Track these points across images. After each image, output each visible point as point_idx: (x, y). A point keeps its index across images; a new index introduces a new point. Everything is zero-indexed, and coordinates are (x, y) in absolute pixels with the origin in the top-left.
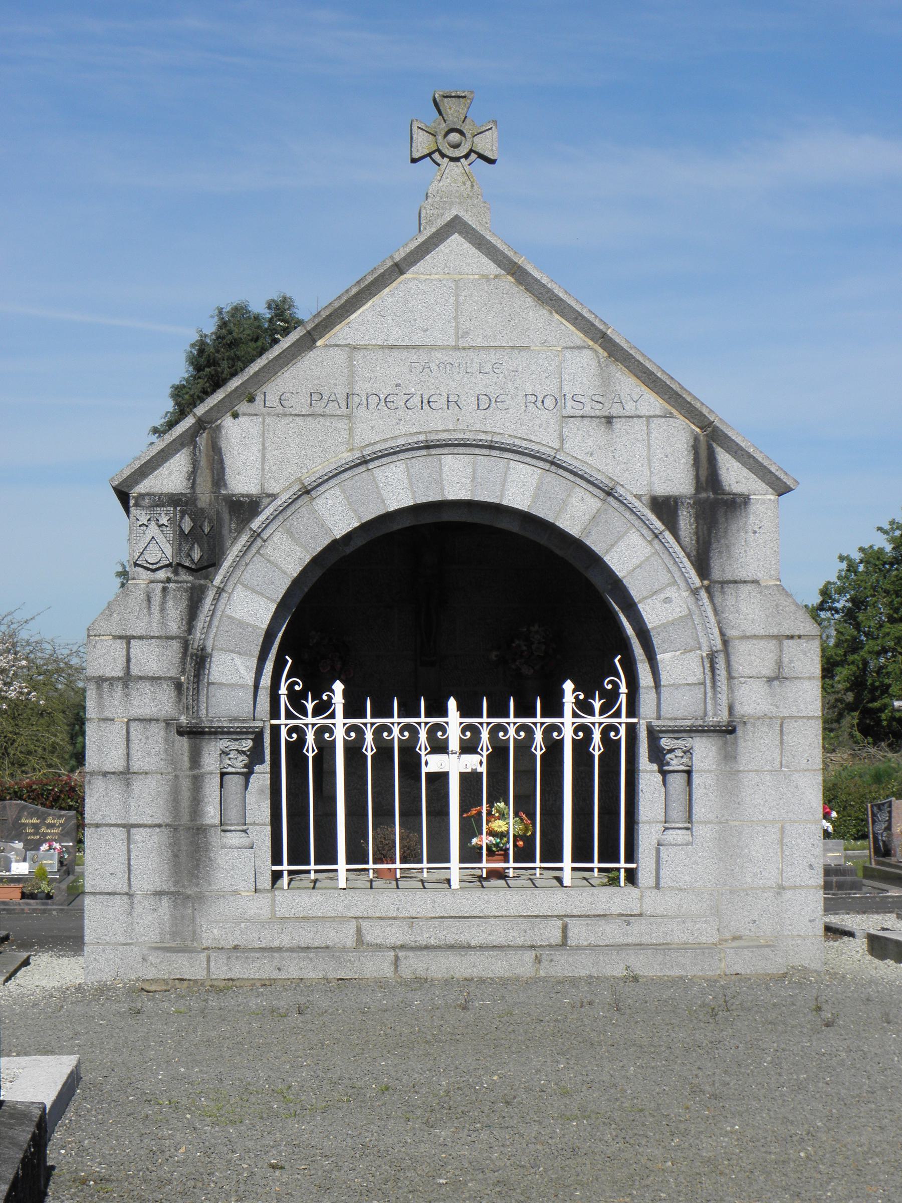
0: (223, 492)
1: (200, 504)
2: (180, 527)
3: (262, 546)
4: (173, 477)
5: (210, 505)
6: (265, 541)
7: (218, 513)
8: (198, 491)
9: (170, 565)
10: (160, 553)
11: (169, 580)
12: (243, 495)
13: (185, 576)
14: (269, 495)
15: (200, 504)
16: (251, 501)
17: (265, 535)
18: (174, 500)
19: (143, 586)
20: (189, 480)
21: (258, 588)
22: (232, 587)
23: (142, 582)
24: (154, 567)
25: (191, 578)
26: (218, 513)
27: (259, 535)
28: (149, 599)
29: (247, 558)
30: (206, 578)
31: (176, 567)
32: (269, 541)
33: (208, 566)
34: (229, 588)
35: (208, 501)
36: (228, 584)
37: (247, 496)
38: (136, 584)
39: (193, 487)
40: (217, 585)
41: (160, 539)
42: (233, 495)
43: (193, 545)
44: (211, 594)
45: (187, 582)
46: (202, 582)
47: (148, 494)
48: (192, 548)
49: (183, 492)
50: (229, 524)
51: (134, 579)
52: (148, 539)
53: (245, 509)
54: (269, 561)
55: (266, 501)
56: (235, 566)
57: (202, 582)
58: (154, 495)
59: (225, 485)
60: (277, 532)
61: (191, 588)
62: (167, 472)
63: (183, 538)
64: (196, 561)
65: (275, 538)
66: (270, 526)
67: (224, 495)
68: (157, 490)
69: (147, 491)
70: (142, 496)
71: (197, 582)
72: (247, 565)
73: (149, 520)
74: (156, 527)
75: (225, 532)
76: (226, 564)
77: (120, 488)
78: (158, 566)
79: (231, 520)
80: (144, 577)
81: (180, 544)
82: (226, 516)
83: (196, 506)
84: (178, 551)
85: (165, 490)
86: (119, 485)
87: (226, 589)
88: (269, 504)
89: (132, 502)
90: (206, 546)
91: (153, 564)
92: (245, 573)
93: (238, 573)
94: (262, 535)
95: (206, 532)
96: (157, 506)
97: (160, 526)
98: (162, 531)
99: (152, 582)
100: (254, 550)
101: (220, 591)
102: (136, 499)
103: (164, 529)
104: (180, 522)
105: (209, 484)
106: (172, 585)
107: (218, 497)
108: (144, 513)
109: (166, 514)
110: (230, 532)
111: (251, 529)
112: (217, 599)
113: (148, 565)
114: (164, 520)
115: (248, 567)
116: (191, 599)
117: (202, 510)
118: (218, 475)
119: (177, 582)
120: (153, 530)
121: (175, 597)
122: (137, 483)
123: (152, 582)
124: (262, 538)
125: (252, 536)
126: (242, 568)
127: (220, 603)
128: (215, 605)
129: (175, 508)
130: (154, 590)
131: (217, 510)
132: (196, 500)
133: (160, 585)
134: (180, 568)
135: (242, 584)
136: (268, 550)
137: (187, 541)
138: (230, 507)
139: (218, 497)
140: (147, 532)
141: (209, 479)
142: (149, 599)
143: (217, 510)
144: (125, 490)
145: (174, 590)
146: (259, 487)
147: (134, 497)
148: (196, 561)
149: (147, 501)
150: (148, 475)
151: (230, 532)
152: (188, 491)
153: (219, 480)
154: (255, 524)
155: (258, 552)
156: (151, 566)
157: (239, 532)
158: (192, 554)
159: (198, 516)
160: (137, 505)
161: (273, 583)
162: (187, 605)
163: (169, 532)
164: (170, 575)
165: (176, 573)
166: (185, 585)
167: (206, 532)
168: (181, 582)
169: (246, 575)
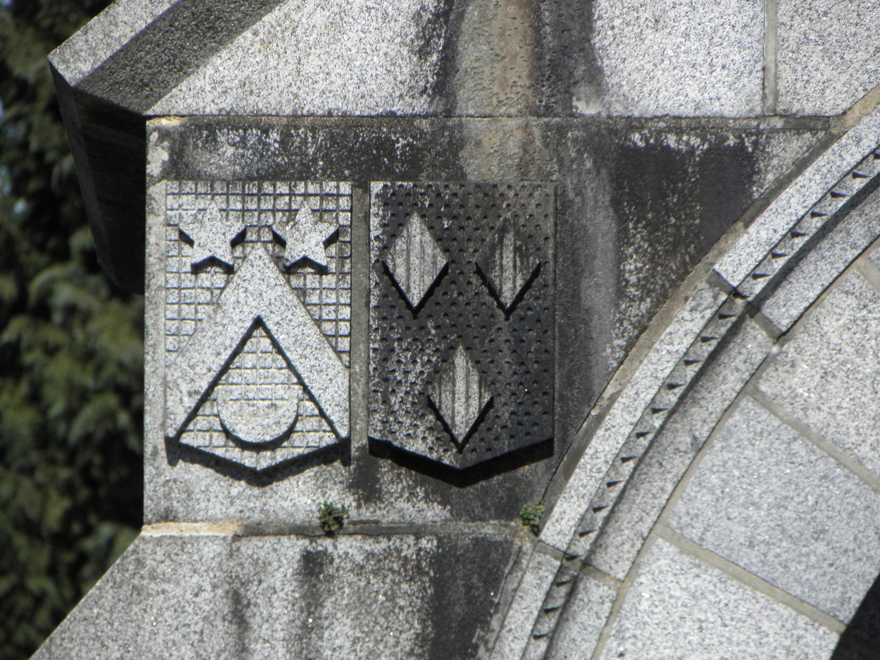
0: (587, 108)
1: (479, 167)
2: (386, 272)
3: (768, 360)
4: (350, 39)
5: (523, 168)
6: (781, 337)
7: (562, 206)
8: (469, 101)
9: (338, 451)
10: (289, 400)
11: (332, 523)
12: (677, 124)
13: (408, 504)
14: (799, 124)
15: (479, 167)
16: (717, 151)
17: (782, 310)
18: (355, 149)
19: (210, 550)
20: (423, 53)
21: (750, 558)
22: (629, 552)
23: (203, 530)
24: (265, 460)
25: (434, 513)
26: (562, 206)
27: (754, 308)
28: (239, 612)
29: (700, 418)
30: (508, 509)
31: (367, 460)
32: (801, 338)
33: (514, 455)
34: (615, 559)
35: (513, 147)
36: (613, 539)
37: (700, 125)
38: (182, 542)
39: (443, 85)
40: (561, 542)
41: (293, 326)
42: (634, 123)
43: (447, 357)
44: (531, 587)
45: (418, 532)
46: (489, 529)
47: (232, 121)
48: (440, 372)
49: (399, 108)
50: (612, 260)
51: (168, 516)
52: (236, 332)
53: (687, 186)
54: (803, 431)
55: (786, 150)
56: (643, 453)
57: (489, 529)
58: (260, 123)
59: (595, 77)
60: (836, 297)
61: (439, 560)
62: (320, 18)
63: (404, 327)
64: (461, 430)
65: (830, 325)
66: (807, 266)
67: (588, 123)
68: (275, 97)
69: (227, 103)
70: (204, 128)
71: (468, 530)
72: (699, 447)
73: (239, 240)
74: (272, 273)
75: (597, 293)
76: (603, 447)
77: (99, 91)
78: (281, 455)
79: (623, 238)
80: (216, 509)
81: (386, 354)
82: (599, 223)
83: (460, 176)
84: (377, 385)
85: (314, 102)
86: (98, 75)
87: (602, 560)
88: (801, 166)
89: (157, 158)
90: (506, 359)
91: (258, 447)
92: (690, 488)
93: (658, 484)
94: (769, 309)
95: (508, 297)
96: (276, 175)
97: (289, 270)
98: (302, 293)
99: (254, 530)
100: (730, 378)
101: (574, 572)
102: (179, 143)
103: (311, 280)
104: (385, 248)
105: (520, 72)
106: (347, 548)
107: (561, 130)
108: (214, 207)
109: (320, 214)
110: (621, 293)
111: (717, 281)
112: (558, 610)
113: (235, 454)
114: (308, 241)
115: (707, 460)
116: (436, 610)
117: (489, 193)
118: (561, 29)
119: (371, 530)
120: (259, 288)
121: (361, 601)
122: (181, 67)
123: (254, 530)
124: (767, 324)
125: (720, 315)
126: (678, 464)
127: (573, 630)
128: (552, 638)
129: (362, 185)
130: (262, 567)
131: (560, 195)
132: (456, 145)
133: (293, 549)
134: (385, 468)
135: (678, 539)
136: (798, 379)
137: (419, 341)
138: (617, 180)
139: (561, 130)
140: (229, 297)
141: (518, 47)
142: (239, 612)
143: (560, 195)
144: (125, 99)
145: (359, 570)
146: (752, 84)
147: (165, 134)
148: (461, 430)
149: (226, 155)
150: (232, 34)
151: (621, 293)
152: (421, 105)
153: (564, 50)
154: (739, 257)
155: (749, 387)
156: (248, 459)
157: (663, 295)
158: (444, 400)
159: (465, 219)
160: (178, 169)
161: (820, 533)
162: (421, 639)
163: (333, 295)
164: (338, 496)
165: (366, 488)
166: (408, 546)
167: (508, 297)
168: (389, 532)
169: (697, 500)
